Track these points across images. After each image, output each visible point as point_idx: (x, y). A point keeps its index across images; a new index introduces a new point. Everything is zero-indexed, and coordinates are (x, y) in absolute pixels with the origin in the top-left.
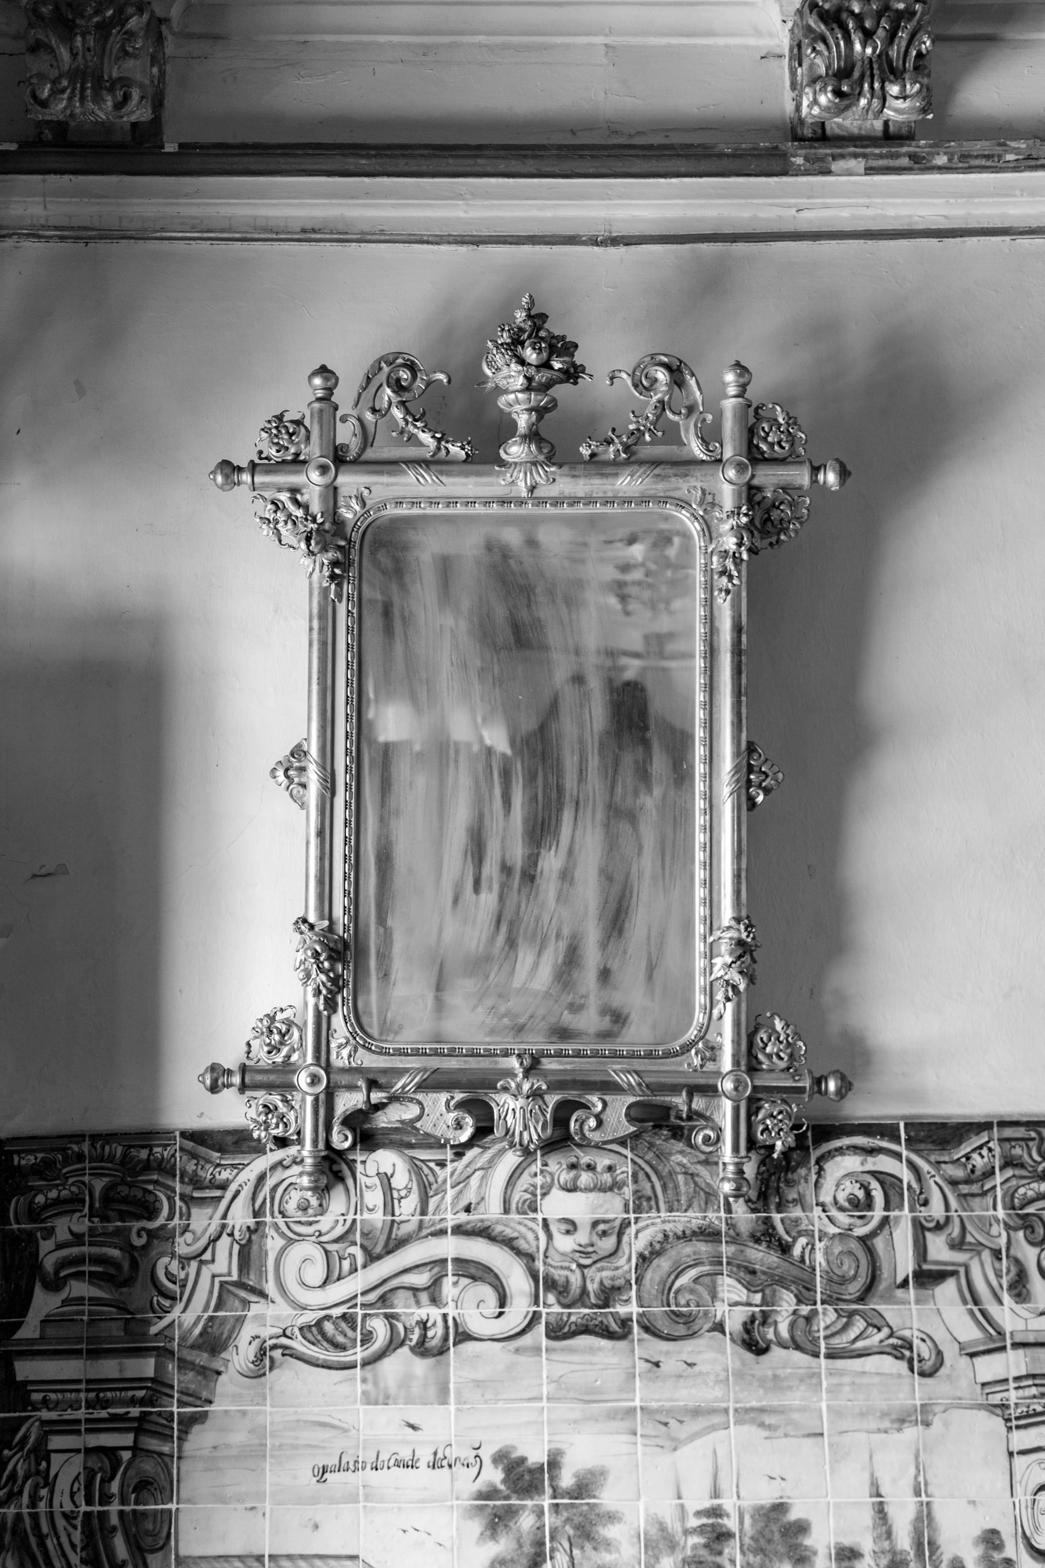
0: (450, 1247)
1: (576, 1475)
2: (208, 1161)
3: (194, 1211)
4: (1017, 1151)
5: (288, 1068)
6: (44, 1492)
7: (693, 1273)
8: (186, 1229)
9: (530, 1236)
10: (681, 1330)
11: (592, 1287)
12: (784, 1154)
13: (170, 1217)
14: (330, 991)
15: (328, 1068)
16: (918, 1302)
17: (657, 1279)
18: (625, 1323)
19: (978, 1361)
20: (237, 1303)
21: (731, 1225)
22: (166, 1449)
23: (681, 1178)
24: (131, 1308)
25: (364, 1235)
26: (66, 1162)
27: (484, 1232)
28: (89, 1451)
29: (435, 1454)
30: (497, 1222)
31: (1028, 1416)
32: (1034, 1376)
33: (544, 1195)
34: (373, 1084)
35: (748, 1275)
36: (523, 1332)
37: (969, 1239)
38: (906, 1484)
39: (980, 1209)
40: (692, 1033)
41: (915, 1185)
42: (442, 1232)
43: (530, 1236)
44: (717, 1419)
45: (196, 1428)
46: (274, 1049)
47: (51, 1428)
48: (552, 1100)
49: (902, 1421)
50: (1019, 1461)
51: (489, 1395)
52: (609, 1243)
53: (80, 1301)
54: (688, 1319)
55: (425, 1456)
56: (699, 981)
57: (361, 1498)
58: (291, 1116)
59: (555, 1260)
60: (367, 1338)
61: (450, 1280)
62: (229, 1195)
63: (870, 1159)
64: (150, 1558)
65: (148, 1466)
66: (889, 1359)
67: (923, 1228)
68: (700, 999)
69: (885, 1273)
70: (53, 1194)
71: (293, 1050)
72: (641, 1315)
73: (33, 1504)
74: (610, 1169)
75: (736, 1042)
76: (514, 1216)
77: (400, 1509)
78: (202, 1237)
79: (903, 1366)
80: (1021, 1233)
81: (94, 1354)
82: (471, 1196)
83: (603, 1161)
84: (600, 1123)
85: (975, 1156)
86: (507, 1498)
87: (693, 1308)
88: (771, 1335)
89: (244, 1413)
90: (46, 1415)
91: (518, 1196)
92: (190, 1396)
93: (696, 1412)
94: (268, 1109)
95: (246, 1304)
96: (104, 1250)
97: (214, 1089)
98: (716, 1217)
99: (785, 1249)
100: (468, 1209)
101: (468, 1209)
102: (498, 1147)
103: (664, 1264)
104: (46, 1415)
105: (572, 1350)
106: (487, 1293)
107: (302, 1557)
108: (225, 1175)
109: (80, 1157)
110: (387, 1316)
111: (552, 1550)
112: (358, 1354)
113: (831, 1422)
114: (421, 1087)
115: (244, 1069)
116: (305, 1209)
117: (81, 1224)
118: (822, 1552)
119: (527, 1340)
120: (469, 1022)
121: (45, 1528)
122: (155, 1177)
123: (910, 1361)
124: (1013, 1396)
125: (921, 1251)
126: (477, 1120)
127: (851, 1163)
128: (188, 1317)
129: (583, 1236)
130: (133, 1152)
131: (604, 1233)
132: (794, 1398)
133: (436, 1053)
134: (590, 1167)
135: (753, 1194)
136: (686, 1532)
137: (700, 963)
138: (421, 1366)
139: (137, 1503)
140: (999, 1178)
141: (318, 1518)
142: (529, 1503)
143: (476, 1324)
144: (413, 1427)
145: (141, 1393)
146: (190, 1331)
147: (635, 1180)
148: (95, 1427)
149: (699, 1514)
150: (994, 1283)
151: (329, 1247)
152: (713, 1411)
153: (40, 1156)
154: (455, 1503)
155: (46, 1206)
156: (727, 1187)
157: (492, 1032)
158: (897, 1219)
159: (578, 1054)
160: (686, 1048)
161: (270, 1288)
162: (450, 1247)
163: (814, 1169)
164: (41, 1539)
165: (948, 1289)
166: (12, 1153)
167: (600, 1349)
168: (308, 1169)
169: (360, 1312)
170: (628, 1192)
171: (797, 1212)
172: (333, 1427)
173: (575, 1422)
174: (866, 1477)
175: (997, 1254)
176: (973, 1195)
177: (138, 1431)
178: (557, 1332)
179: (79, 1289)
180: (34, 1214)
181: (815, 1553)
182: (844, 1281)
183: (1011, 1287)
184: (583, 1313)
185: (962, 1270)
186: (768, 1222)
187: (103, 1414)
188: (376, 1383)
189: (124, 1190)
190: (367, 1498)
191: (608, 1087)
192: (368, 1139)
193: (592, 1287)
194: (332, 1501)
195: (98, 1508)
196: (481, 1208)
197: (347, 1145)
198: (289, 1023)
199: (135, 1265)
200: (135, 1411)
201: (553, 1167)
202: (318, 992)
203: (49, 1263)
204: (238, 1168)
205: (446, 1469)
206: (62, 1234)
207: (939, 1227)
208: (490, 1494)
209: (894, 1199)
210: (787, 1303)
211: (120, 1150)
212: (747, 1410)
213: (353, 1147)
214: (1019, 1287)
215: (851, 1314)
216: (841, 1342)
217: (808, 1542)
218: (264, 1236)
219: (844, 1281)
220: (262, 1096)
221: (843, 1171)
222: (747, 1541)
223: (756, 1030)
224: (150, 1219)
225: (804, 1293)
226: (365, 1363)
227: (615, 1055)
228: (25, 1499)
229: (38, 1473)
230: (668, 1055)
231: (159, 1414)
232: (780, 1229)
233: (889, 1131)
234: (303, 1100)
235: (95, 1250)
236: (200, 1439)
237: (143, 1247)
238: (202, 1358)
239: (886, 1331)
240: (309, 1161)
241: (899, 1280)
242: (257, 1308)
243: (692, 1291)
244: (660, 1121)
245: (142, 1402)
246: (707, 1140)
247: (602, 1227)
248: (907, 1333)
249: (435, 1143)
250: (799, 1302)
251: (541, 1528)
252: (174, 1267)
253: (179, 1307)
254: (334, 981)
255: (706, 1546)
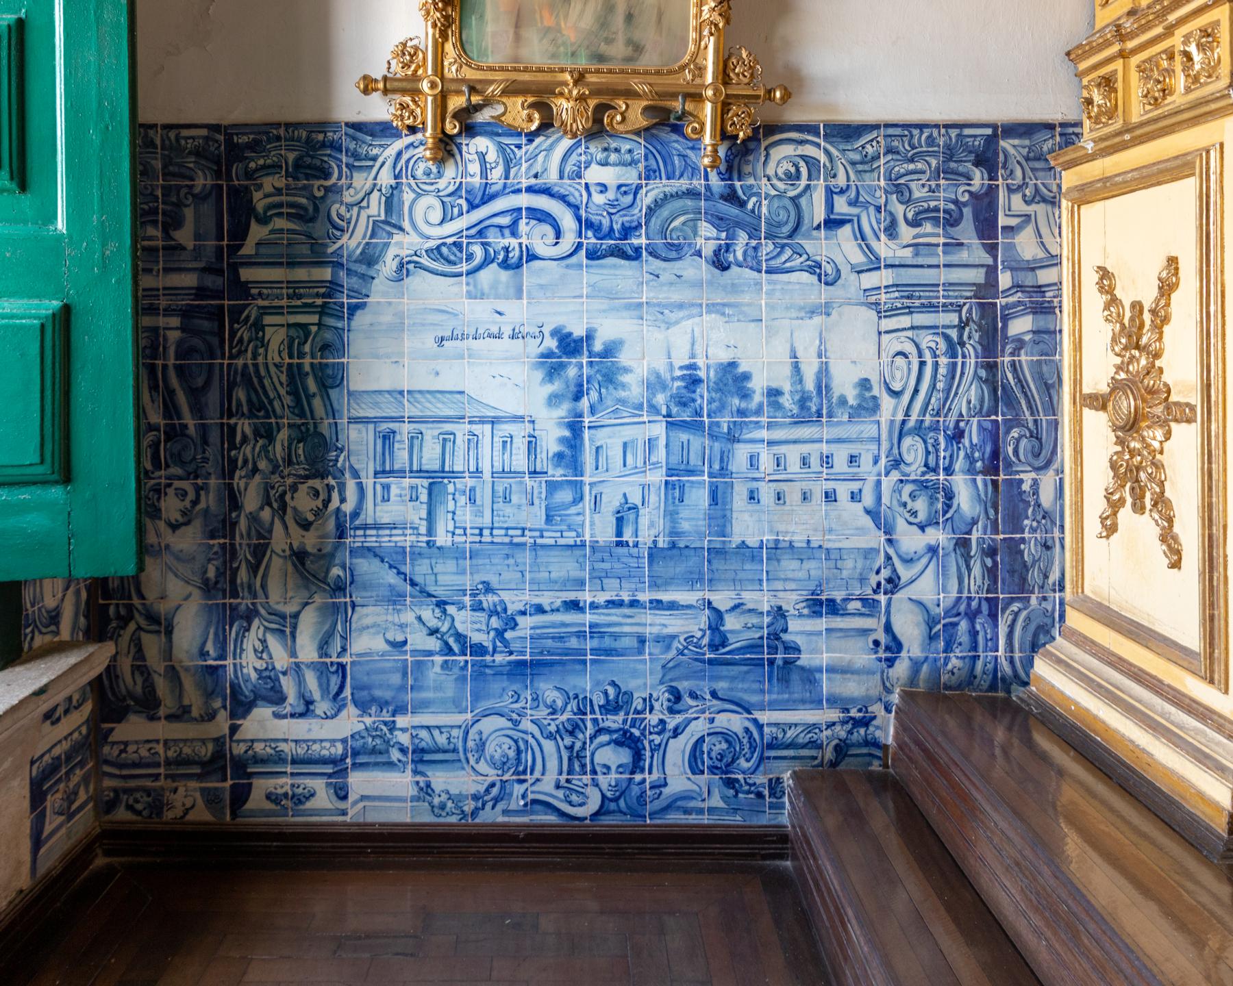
0: (524, 200)
1: (604, 344)
2: (364, 142)
3: (355, 174)
4: (895, 143)
5: (415, 78)
6: (261, 351)
7: (682, 219)
8: (350, 186)
9: (577, 194)
10: (673, 255)
11: (616, 227)
12: (744, 141)
13: (340, 178)
14: (443, 25)
15: (442, 78)
16: (826, 239)
17: (659, 222)
18: (638, 250)
19: (863, 276)
20: (384, 234)
21: (708, 188)
22: (340, 325)
23: (676, 158)
24: (315, 236)
25: (467, 192)
26: (269, 141)
27: (547, 191)
28: (289, 325)
30: (555, 185)
31: (892, 310)
32: (897, 285)
33: (586, 168)
34: (473, 90)
35: (719, 221)
36: (571, 255)
37: (861, 199)
38: (813, 351)
39: (869, 180)
40: (687, 58)
41: (828, 164)
42: (519, 191)
43: (577, 194)
44: (695, 311)
45: (359, 313)
46: (406, 66)
47: (265, 311)
48: (592, 103)
49: (813, 312)
50: (885, 338)
51: (548, 294)
52: (628, 199)
53: (281, 231)
54: (678, 248)
55: (507, 331)
56: (693, 23)
58: (418, 111)
59: (592, 209)
60: (470, 257)
61: (524, 221)
62: (378, 164)
63: (800, 147)
64: (331, 391)
65: (329, 336)
66: (806, 274)
67: (832, 192)
68: (692, 35)
69: (806, 221)
70: (261, 162)
71: (418, 67)
72: (648, 245)
73: (255, 357)
74: (630, 151)
75: (716, 63)
76: (566, 181)
78: (361, 191)
79: (815, 278)
80: (894, 196)
81: (291, 265)
82: (538, 167)
83: (625, 146)
84: (624, 119)
85: (868, 146)
86: (560, 357)
87: (682, 241)
88: (731, 258)
89: (390, 303)
90: (261, 302)
91: (569, 168)
92: (354, 292)
93: (681, 306)
94: (403, 107)
95: (390, 235)
96: (296, 199)
97: (366, 91)
98: (699, 184)
99: (742, 204)
100: (536, 176)
101: (536, 176)
102: (556, 136)
103: (665, 212)
104: (261, 302)
105: (602, 267)
106: (548, 229)
107: (428, 392)
108: (375, 151)
109: (278, 138)
110: (483, 244)
111: (588, 389)
112: (464, 267)
113: (767, 313)
114: (505, 92)
115: (385, 79)
116: (428, 175)
117: (280, 182)
118: (758, 391)
119: (574, 260)
120: (536, 52)
121: (263, 372)
122: (329, 152)
123: (820, 276)
124: (883, 297)
125: (830, 206)
126: (542, 118)
127: (788, 150)
128: (352, 243)
129: (611, 195)
130: (314, 135)
131: (625, 193)
132: (746, 298)
133: (515, 70)
134: (617, 150)
135: (723, 168)
136: (673, 379)
137: (693, 11)
138: (505, 275)
139: (322, 358)
140: (882, 161)
141: (438, 368)
142: (574, 360)
143: (541, 249)
144: (500, 313)
145: (323, 290)
146: (354, 251)
147: (646, 159)
148: (293, 310)
149: (681, 368)
150: (876, 227)
151: (445, 199)
152: (693, 305)
153: (251, 137)
155: (257, 170)
156: (706, 161)
157: (554, 56)
158: (816, 186)
159: (610, 72)
160: (683, 68)
161: (406, 225)
162: (524, 200)
163: (764, 153)
164: (260, 379)
165: (846, 230)
166: (232, 134)
167: (621, 266)
168: (430, 146)
169: (465, 241)
170: (641, 166)
171: (751, 181)
172: (447, 312)
173: (604, 311)
174: (788, 346)
175: (878, 209)
176: (865, 171)
177: (322, 314)
178: (593, 255)
179: (280, 223)
180: (249, 175)
181: (754, 392)
182: (780, 225)
183: (885, 230)
184: (611, 242)
185: (855, 219)
186: (732, 187)
187: (299, 303)
188: (475, 286)
189: (308, 160)
190: (470, 357)
191: (630, 94)
192: (470, 130)
193: (616, 227)
194: (447, 358)
195: (296, 361)
196: (545, 175)
197: (456, 131)
198: (416, 48)
199: (316, 209)
200: (319, 301)
201: (592, 149)
202: (434, 25)
203: (260, 207)
204: (384, 147)
205: (521, 340)
206: (268, 188)
207: (842, 192)
208: (548, 355)
209: (814, 174)
210: (742, 238)
211: (304, 134)
212: (713, 305)
213: (460, 134)
214: (891, 230)
215: (783, 247)
216: (775, 263)
217: (750, 385)
218: (402, 191)
219: (780, 225)
220: (398, 98)
221: (782, 156)
222: (711, 384)
223: (729, 57)
224: (326, 179)
225: (753, 233)
226: (468, 273)
227: (635, 72)
228: (249, 354)
229: (257, 339)
230: (670, 72)
231: (335, 303)
232: (740, 192)
233: (812, 129)
234: (426, 101)
235: (290, 199)
236: (361, 319)
237: (322, 198)
238: (362, 269)
239: (805, 256)
240: (430, 140)
241: (815, 225)
242: (398, 237)
243: (681, 230)
244: (665, 121)
245: (323, 296)
246: (694, 129)
247: (623, 189)
248: (818, 258)
249: (515, 132)
250: (750, 238)
251: (581, 376)
252: (343, 210)
253: (347, 236)
254: (446, 17)
255: (686, 387)
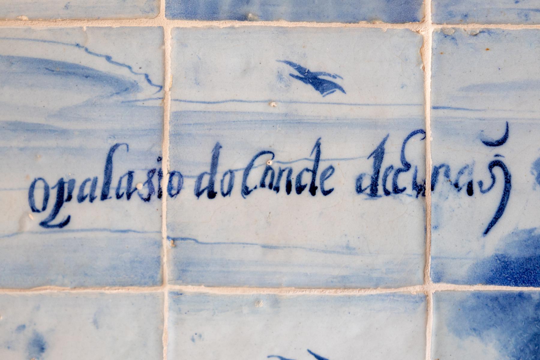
29: (379, 155)
55: (349, 160)
57: (167, 271)
77: (275, 302)
141: (44, 324)
144: (317, 82)
154: (433, 288)
172: (88, 75)
190: (183, 272)
